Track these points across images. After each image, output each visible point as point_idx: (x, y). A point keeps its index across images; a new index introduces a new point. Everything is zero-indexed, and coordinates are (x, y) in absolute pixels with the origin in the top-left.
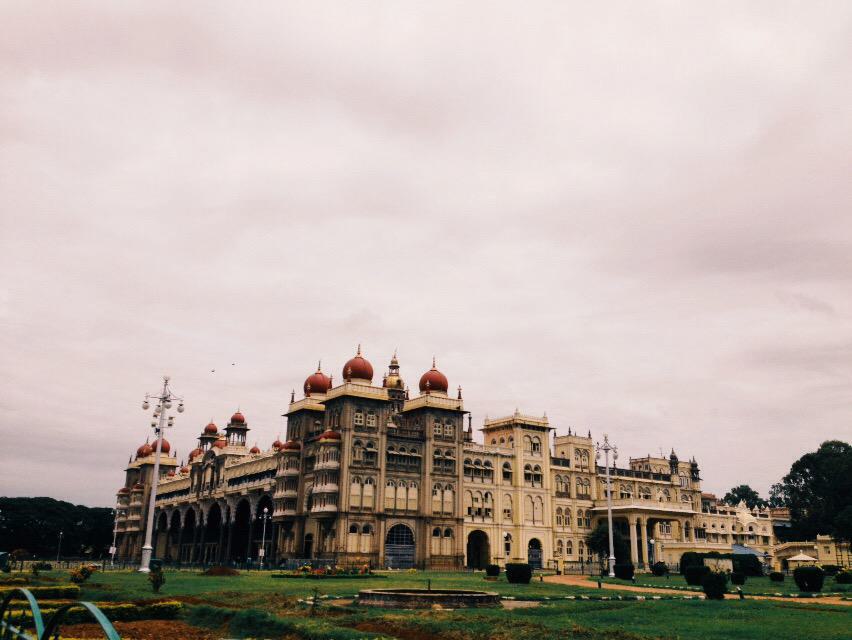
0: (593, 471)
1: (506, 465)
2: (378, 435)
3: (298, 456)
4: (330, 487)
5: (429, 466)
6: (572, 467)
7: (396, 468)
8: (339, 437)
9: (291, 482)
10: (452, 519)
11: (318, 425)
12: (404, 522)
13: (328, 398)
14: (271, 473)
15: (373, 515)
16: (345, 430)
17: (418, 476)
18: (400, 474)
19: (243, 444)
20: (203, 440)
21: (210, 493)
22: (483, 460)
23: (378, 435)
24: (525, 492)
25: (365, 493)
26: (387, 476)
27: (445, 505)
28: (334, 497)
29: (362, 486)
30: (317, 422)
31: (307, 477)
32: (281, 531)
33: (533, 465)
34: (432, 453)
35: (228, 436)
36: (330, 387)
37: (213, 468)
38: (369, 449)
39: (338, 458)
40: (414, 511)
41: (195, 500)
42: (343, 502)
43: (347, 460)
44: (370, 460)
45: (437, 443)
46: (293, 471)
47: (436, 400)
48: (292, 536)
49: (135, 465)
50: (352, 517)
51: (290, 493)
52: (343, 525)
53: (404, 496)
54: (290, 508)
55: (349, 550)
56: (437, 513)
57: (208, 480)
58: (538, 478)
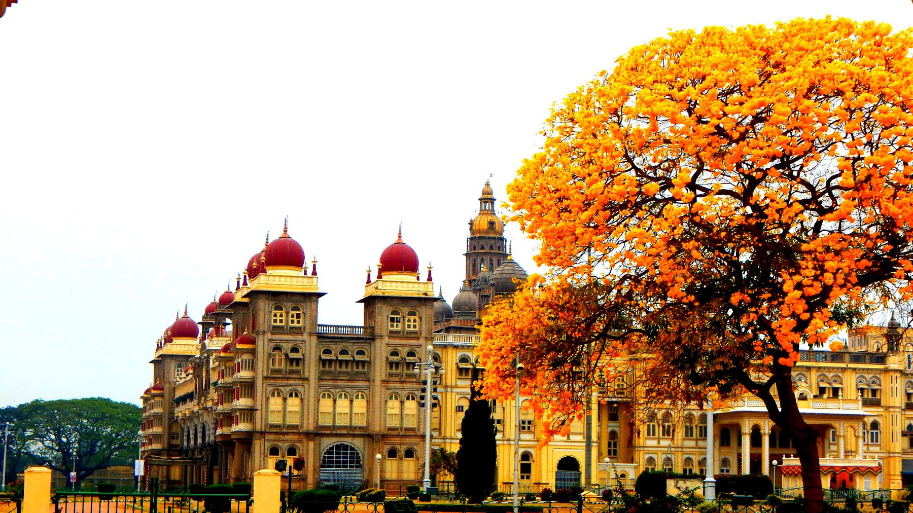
2: (305, 337)
5: (380, 371)
12: (347, 441)
15: (299, 433)
17: (366, 384)
18: (339, 383)
25: (289, 409)
27: (405, 419)
28: (249, 413)
29: (285, 399)
38: (293, 355)
39: (252, 366)
40: (361, 428)
44: (295, 368)
50: (272, 437)
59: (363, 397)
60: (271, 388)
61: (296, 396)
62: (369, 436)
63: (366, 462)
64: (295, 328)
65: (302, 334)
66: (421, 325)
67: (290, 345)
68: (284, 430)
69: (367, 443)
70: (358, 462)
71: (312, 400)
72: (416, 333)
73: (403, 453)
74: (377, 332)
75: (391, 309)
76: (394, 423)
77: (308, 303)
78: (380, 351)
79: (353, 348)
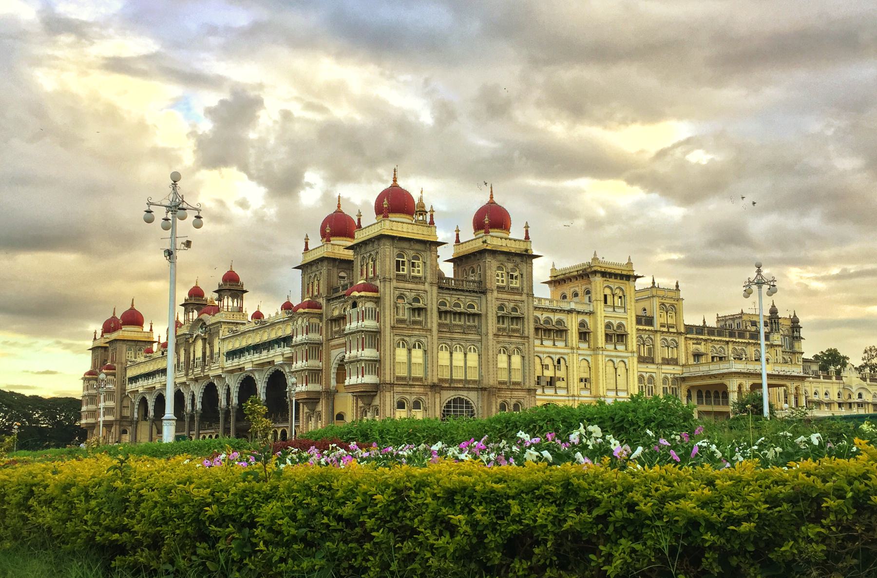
0: (682, 330)
1: (582, 324)
2: (427, 287)
3: (320, 316)
4: (369, 353)
5: (491, 325)
6: (657, 326)
7: (450, 329)
9: (314, 349)
10: (522, 390)
11: (344, 278)
12: (464, 394)
13: (355, 242)
14: (286, 340)
18: (456, 336)
19: (240, 310)
20: (187, 306)
21: (203, 371)
22: (555, 317)
23: (427, 287)
24: (607, 356)
25: (414, 360)
26: (439, 338)
28: (375, 365)
29: (409, 350)
30: (342, 274)
31: (333, 343)
32: (304, 410)
33: (615, 322)
34: (495, 309)
35: (220, 300)
36: (359, 227)
37: (204, 340)
38: (416, 305)
39: (377, 317)
40: (474, 382)
41: (184, 379)
42: (388, 371)
43: (389, 318)
46: (314, 336)
47: (495, 240)
48: (319, 416)
49: (101, 342)
50: (400, 389)
51: (314, 363)
53: (462, 364)
54: (314, 381)
56: (504, 383)
57: (199, 354)
58: (622, 337)
59: (475, 351)
61: (419, 347)
62: (484, 389)
66: (522, 282)
68: (411, 383)
72: (517, 289)
77: (428, 253)
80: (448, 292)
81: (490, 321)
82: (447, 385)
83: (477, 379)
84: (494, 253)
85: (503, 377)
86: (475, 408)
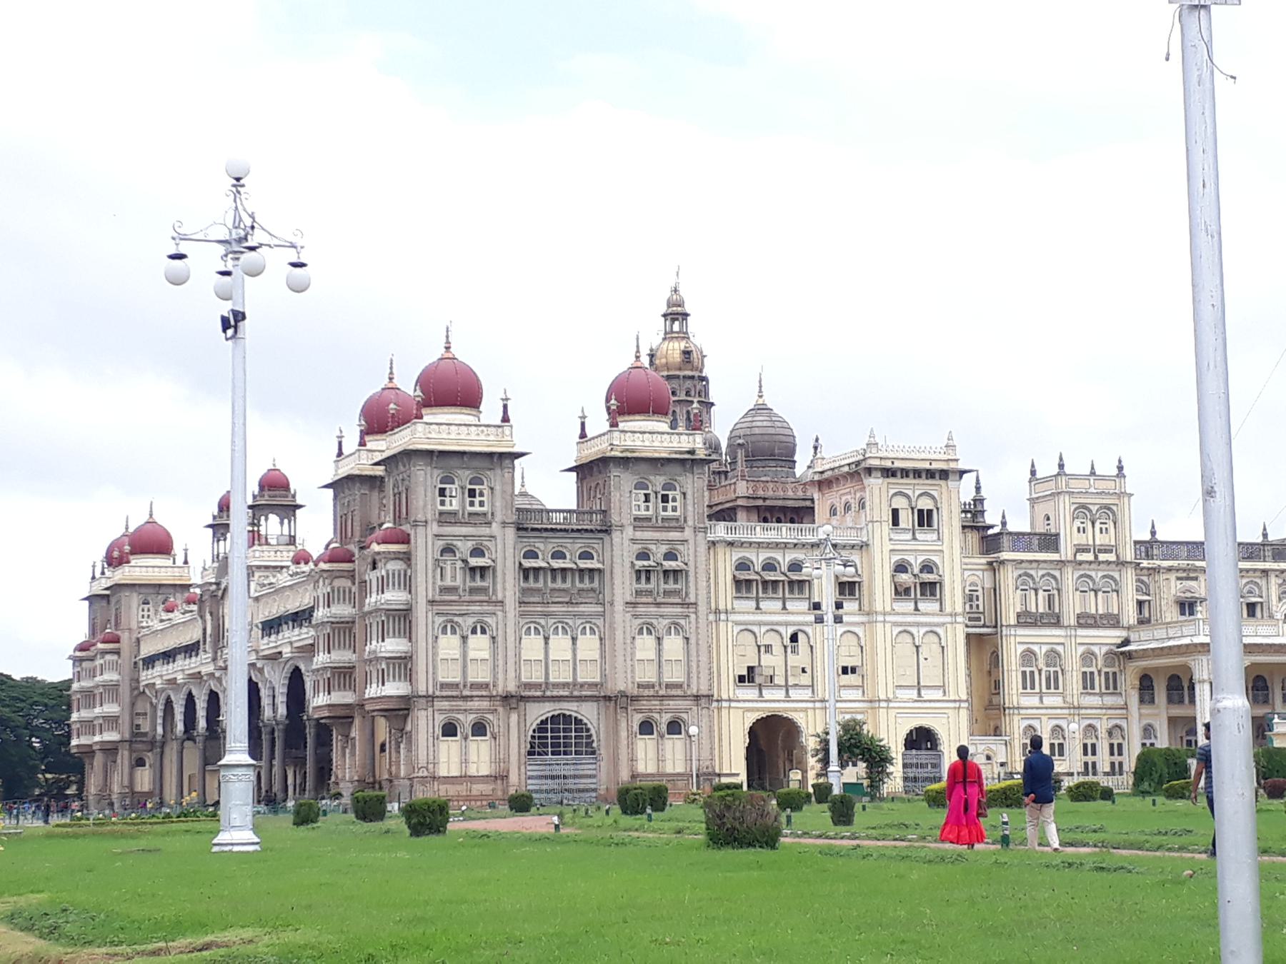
5: (622, 586)
8: (405, 540)
12: (570, 708)
16: (415, 524)
17: (600, 609)
18: (553, 608)
24: (895, 624)
25: (472, 654)
28: (403, 665)
29: (464, 639)
33: (916, 562)
38: (474, 562)
44: (479, 583)
45: (639, 535)
52: (424, 723)
55: (443, 772)
58: (930, 589)
60: (442, 619)
61: (483, 632)
62: (607, 698)
63: (603, 743)
64: (476, 514)
65: (489, 524)
67: (470, 545)
69: (603, 711)
70: (589, 744)
71: (511, 639)
73: (664, 728)
74: (615, 518)
75: (635, 479)
76: (647, 674)
77: (499, 471)
78: (620, 553)
79: (573, 547)
80: (537, 534)
81: (617, 581)
82: (539, 694)
83: (598, 680)
84: (625, 462)
85: (649, 675)
86: (593, 732)
